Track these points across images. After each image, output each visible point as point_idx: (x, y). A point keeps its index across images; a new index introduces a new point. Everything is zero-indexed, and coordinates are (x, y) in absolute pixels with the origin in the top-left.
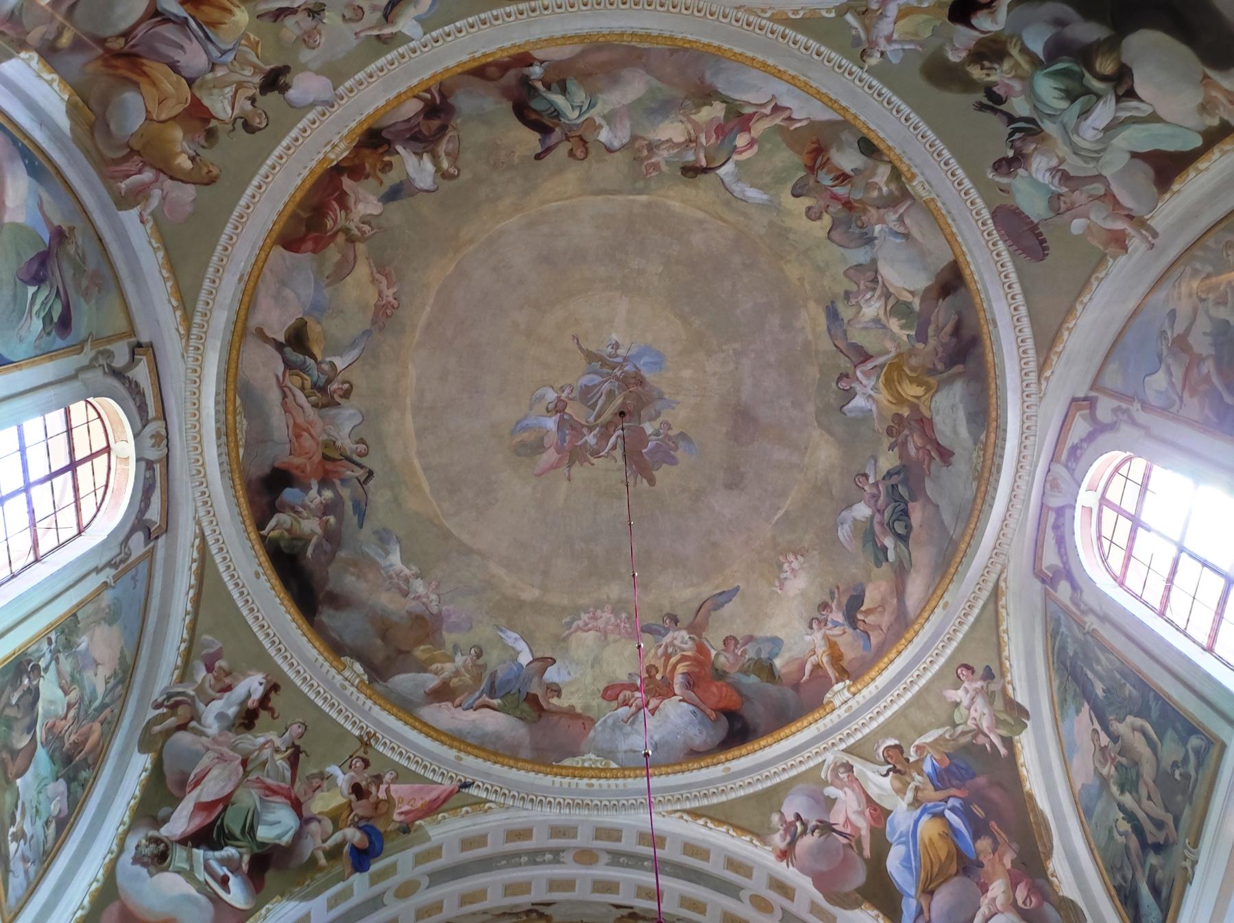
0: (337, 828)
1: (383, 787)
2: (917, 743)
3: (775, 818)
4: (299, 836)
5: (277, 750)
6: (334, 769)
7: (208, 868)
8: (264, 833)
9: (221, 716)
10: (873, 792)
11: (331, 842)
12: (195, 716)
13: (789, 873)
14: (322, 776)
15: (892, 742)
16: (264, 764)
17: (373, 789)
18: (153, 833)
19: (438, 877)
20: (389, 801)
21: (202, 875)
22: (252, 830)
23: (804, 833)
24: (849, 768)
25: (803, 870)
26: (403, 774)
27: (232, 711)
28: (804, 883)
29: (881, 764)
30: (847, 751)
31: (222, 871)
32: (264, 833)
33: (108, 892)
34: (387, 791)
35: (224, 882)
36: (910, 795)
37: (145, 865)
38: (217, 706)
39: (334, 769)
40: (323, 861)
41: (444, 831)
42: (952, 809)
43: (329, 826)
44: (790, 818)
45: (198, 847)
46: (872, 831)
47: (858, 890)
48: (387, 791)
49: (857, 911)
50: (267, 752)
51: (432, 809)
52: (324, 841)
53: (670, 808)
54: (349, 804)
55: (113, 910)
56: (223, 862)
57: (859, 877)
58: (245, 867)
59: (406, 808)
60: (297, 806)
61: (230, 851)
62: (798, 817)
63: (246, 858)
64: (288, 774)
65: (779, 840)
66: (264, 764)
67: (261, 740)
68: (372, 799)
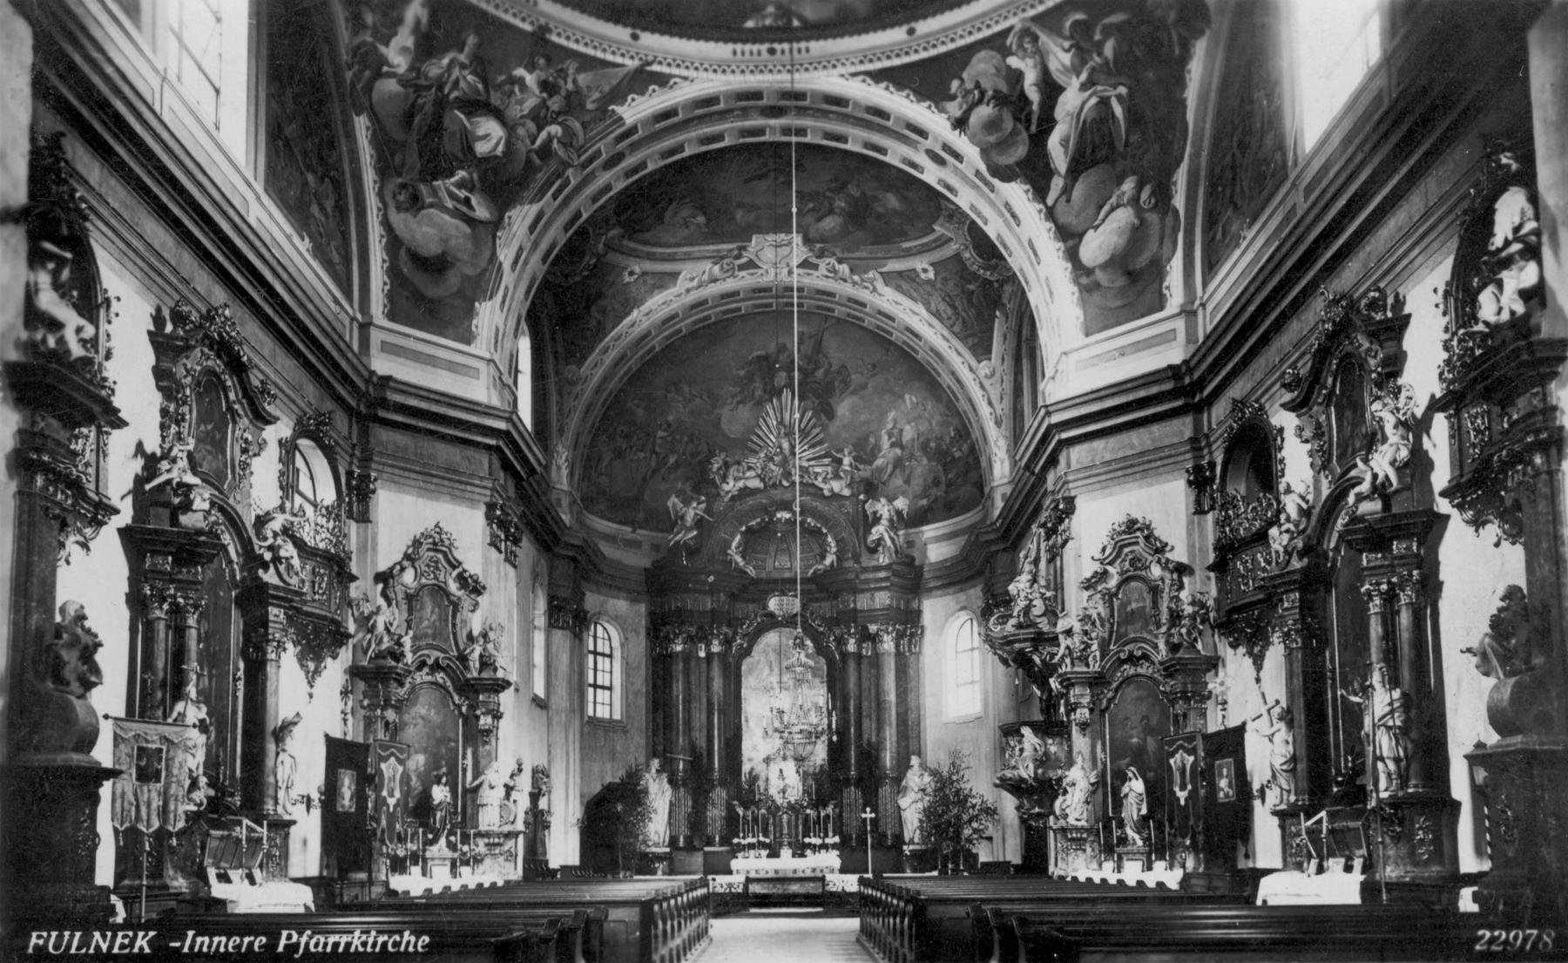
0: (540, 128)
1: (570, 80)
2: (1107, 21)
3: (955, 84)
4: (509, 144)
5: (463, 66)
6: (520, 72)
7: (453, 196)
8: (482, 148)
9: (404, 50)
10: (1053, 66)
11: (539, 142)
12: (384, 61)
13: (961, 142)
14: (514, 81)
15: (1079, 16)
16: (457, 82)
17: (561, 82)
18: (400, 180)
19: (634, 147)
20: (578, 91)
21: (450, 204)
22: (471, 149)
23: (980, 101)
24: (1035, 39)
25: (973, 140)
26: (588, 63)
27: (410, 42)
28: (971, 152)
29: (1066, 38)
30: (1034, 19)
31: (462, 194)
32: (482, 148)
33: (394, 243)
34: (575, 81)
35: (467, 201)
36: (1084, 76)
37: (407, 210)
38: (396, 42)
39: (520, 72)
40: (538, 162)
41: (636, 110)
42: (1119, 97)
43: (531, 125)
44: (969, 85)
45: (435, 179)
46: (1042, 104)
47: (1018, 164)
48: (575, 81)
49: (1013, 184)
50: (456, 73)
51: (619, 94)
52: (533, 142)
53: (853, 69)
54: (544, 101)
55: (403, 252)
56: (460, 185)
57: (1020, 151)
58: (478, 185)
59: (596, 95)
60: (498, 115)
61: (461, 174)
62: (978, 85)
63: (475, 176)
64: (480, 86)
65: (955, 108)
66: (457, 82)
67: (445, 61)
68: (563, 93)
